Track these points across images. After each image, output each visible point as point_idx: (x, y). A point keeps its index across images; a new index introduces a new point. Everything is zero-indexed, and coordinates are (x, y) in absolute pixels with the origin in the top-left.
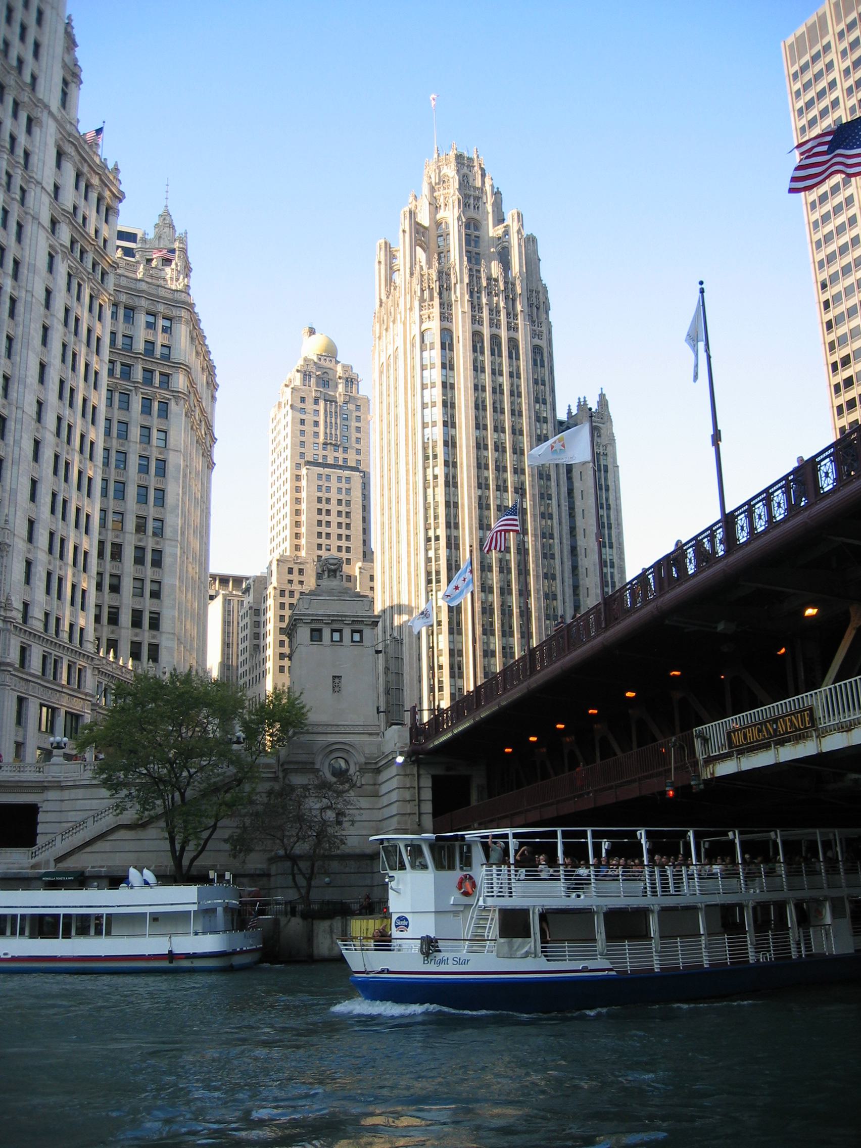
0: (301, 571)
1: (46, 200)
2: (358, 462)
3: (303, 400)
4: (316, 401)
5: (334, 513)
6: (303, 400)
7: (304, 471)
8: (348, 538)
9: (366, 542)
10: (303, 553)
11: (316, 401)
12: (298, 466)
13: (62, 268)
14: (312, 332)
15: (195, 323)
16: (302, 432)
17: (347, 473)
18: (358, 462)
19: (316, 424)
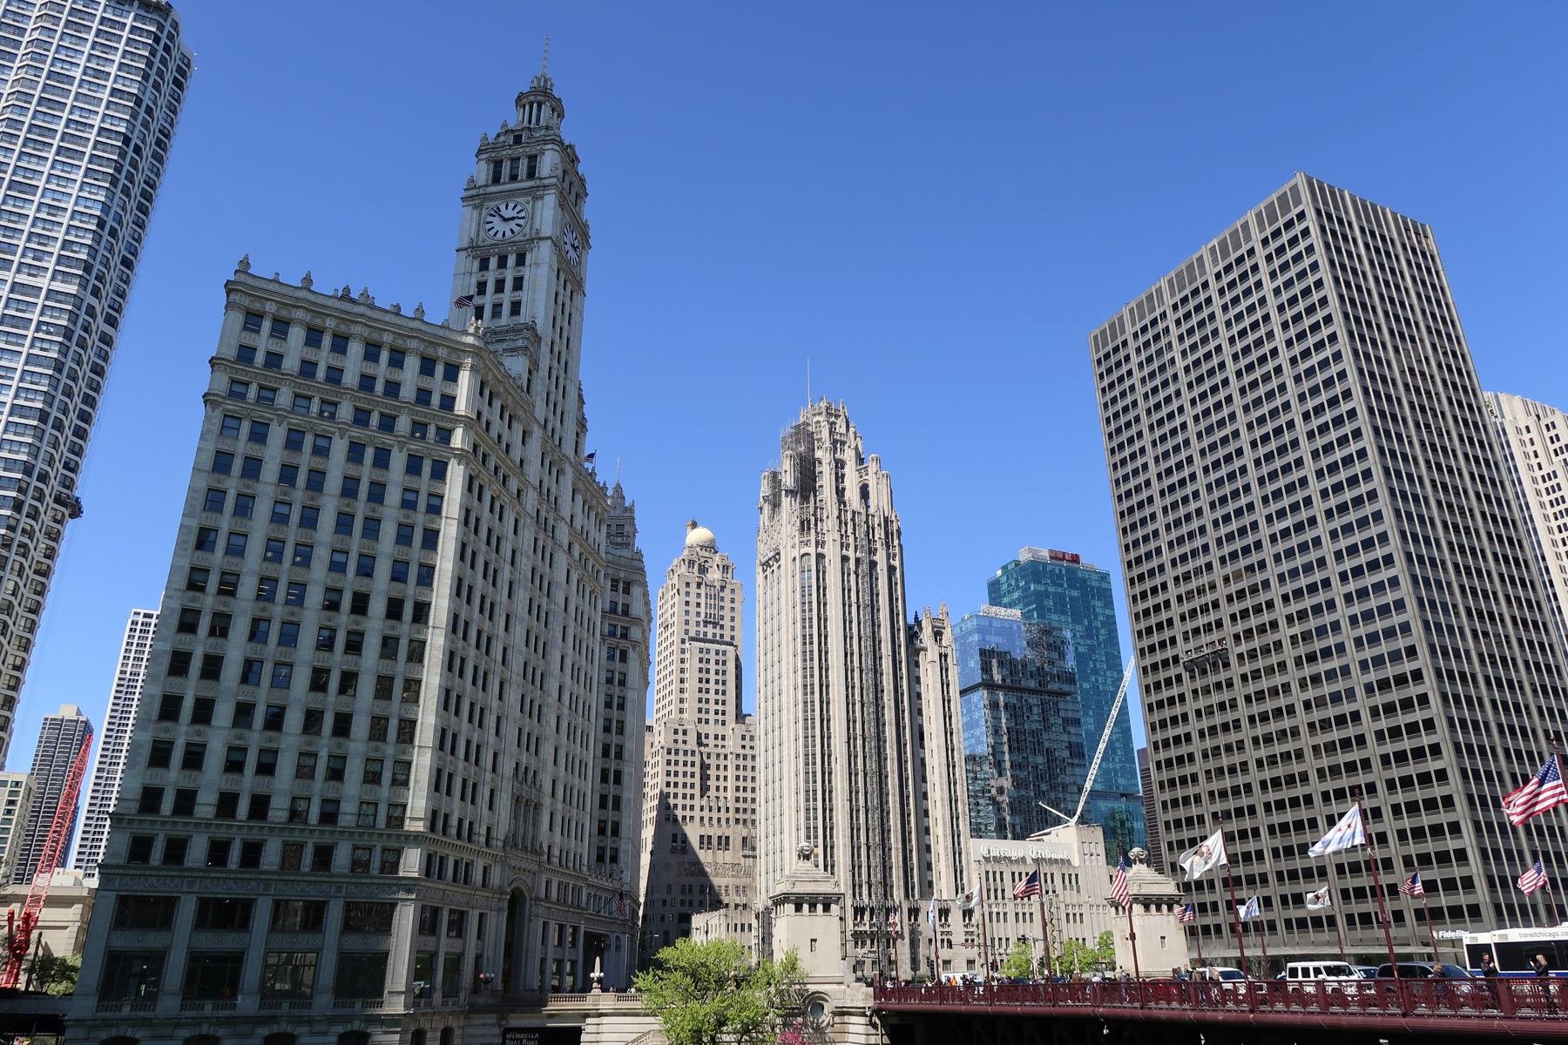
0: (685, 732)
1: (566, 529)
2: (733, 638)
3: (688, 584)
4: (699, 585)
5: (712, 682)
6: (688, 584)
7: (687, 645)
8: (724, 703)
9: (738, 706)
10: (685, 716)
11: (699, 585)
12: (683, 641)
13: (574, 577)
14: (694, 525)
15: (644, 585)
16: (687, 612)
17: (723, 647)
18: (733, 638)
19: (698, 605)
